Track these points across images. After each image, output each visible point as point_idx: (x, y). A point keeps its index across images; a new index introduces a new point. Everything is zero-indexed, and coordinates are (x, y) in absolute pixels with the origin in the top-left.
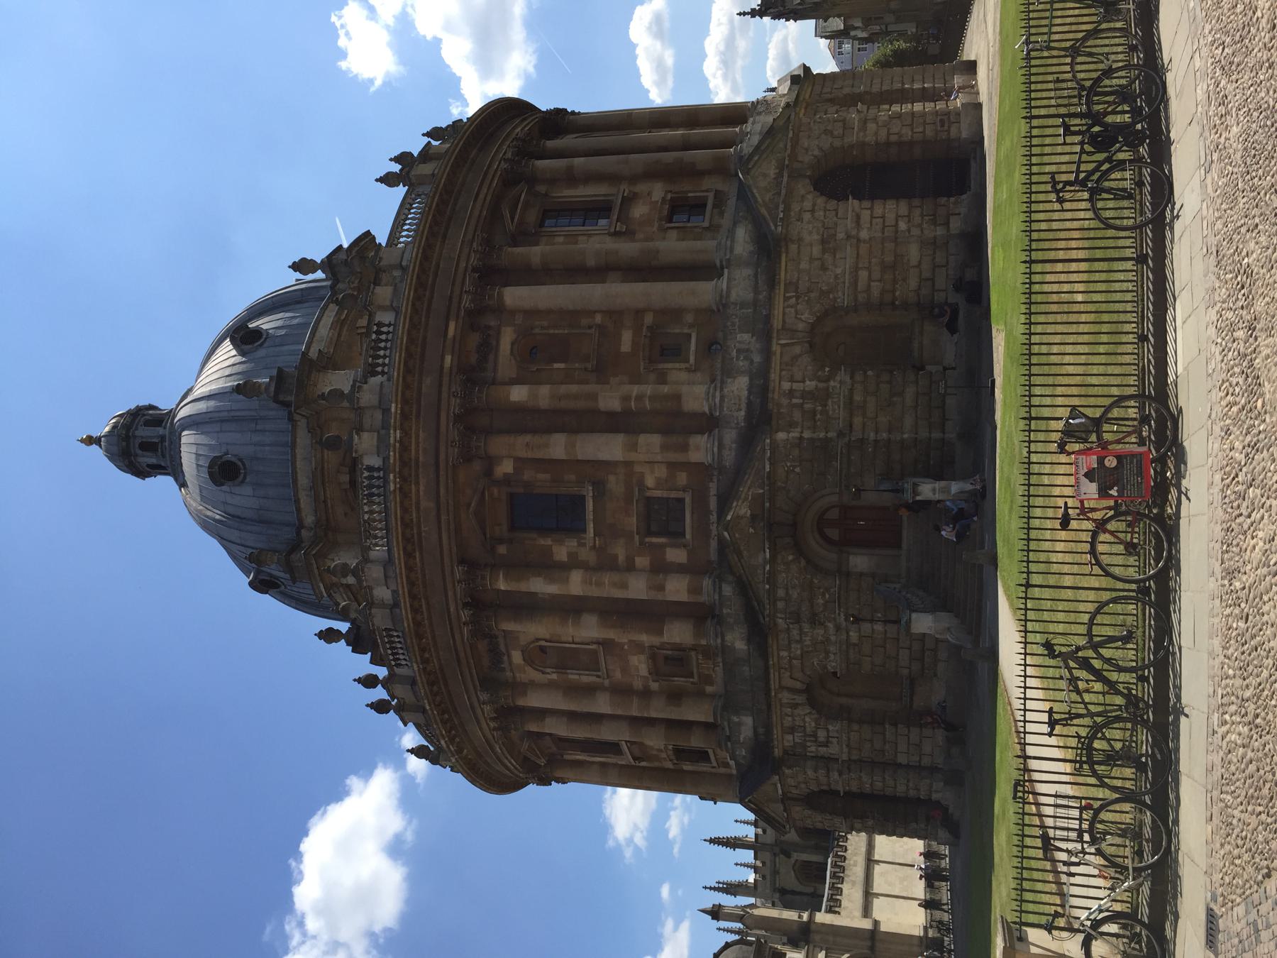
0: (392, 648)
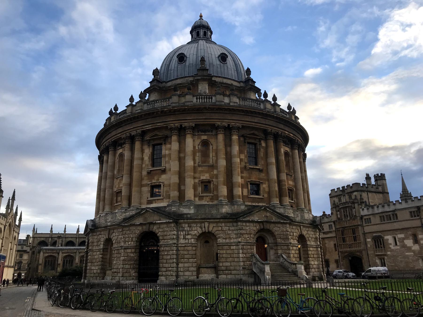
0: (204, 98)
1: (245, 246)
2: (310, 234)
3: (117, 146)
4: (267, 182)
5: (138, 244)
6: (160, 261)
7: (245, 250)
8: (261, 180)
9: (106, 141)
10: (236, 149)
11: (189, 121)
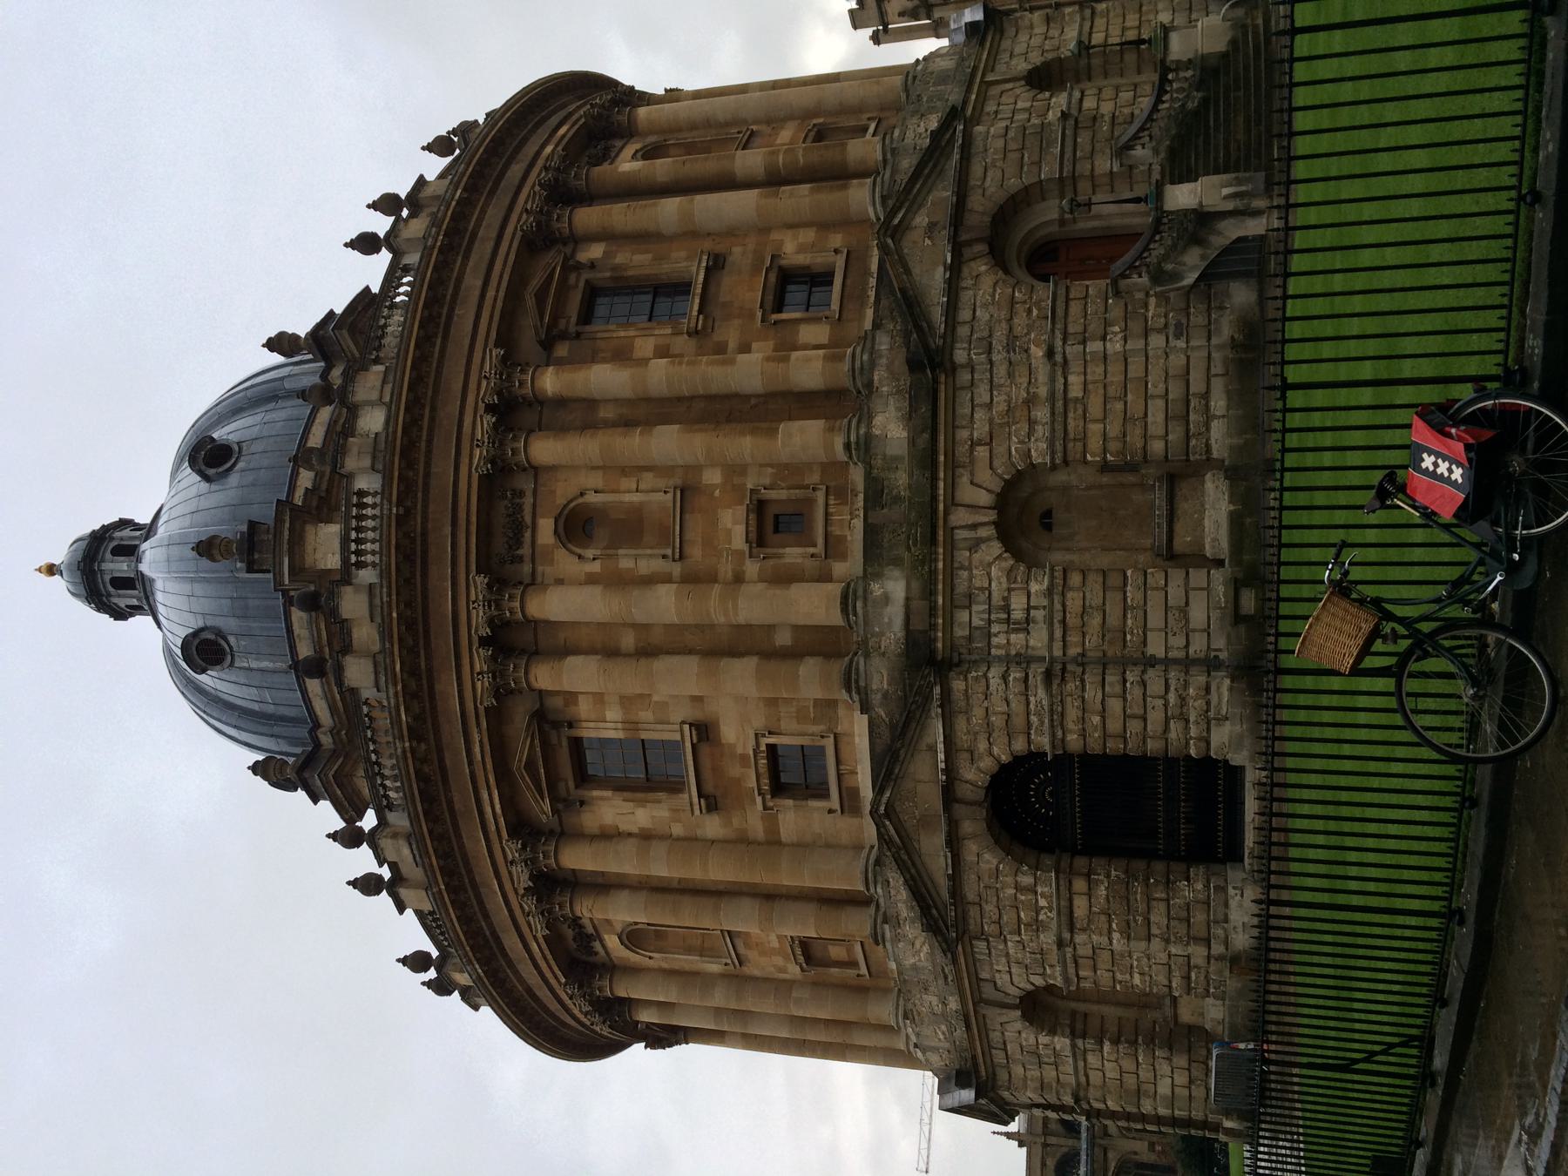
0: (358, 529)
1: (1071, 329)
2: (1029, 44)
3: (591, 959)
4: (775, 236)
5: (1048, 860)
6: (1133, 748)
7: (1091, 328)
8: (763, 262)
9: (567, 1010)
10: (604, 379)
11: (464, 603)
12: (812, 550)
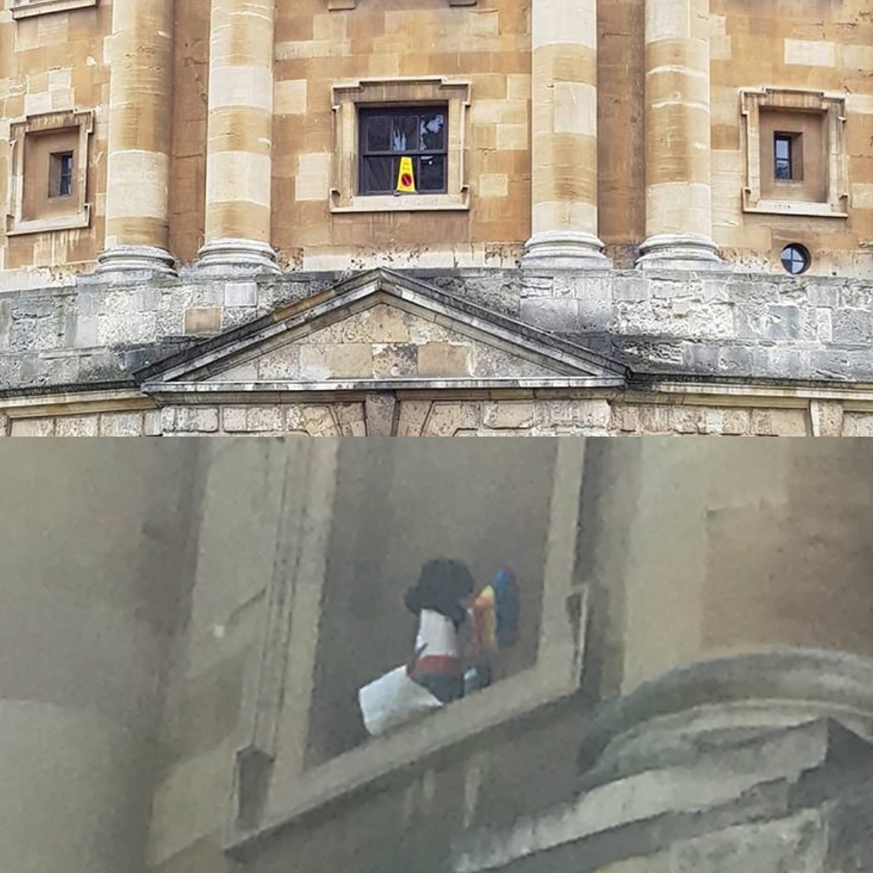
4: (515, 81)
12: (18, 215)
